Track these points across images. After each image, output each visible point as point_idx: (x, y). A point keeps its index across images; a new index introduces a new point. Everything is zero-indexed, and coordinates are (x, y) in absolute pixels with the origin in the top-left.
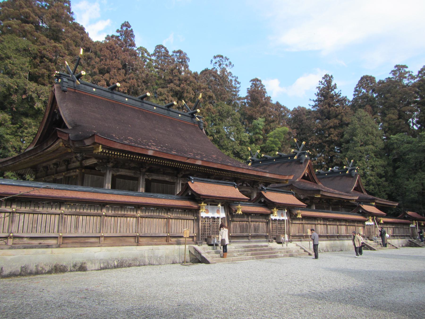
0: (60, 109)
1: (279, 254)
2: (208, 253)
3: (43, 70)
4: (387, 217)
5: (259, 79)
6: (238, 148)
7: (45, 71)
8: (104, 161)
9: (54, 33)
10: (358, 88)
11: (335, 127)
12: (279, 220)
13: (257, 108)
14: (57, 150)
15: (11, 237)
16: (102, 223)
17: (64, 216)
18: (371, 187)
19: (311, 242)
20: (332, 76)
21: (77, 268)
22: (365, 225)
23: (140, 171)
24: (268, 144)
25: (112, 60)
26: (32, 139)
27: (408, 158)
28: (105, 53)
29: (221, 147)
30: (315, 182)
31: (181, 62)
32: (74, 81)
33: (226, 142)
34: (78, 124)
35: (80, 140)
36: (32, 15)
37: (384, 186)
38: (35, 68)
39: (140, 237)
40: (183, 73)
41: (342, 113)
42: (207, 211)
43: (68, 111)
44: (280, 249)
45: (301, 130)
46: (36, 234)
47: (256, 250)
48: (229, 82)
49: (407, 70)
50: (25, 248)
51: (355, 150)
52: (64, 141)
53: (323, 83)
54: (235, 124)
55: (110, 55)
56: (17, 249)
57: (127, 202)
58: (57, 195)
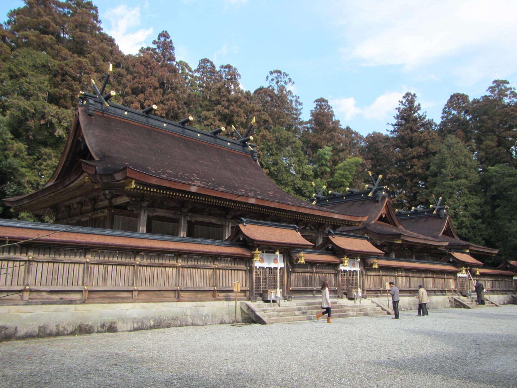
0: (85, 137)
1: (351, 313)
2: (264, 311)
3: (65, 90)
4: (484, 267)
5: (326, 99)
6: (300, 183)
7: (68, 91)
8: (138, 199)
9: (78, 45)
10: (447, 109)
11: (419, 157)
12: (350, 271)
13: (323, 135)
14: (82, 186)
15: (27, 291)
16: (135, 275)
17: (90, 265)
18: (465, 230)
19: (391, 299)
20: (414, 95)
21: (106, 328)
22: (457, 277)
23: (181, 212)
24: (336, 178)
25: (147, 78)
26: (52, 173)
27: (510, 195)
28: (139, 69)
29: (279, 182)
30: (395, 225)
31: (231, 79)
32: (102, 103)
33: (285, 176)
34: (106, 154)
35: (110, 174)
36: (52, 24)
37: (480, 230)
38: (55, 88)
39: (182, 291)
40: (233, 93)
41: (427, 139)
42: (262, 260)
43: (94, 139)
44: (352, 307)
45: (377, 162)
46: (57, 287)
48: (288, 103)
49: (508, 86)
50: (43, 304)
51: (444, 186)
52: (90, 175)
53: (404, 103)
54: (296, 154)
55: (145, 72)
56: (34, 305)
57: (166, 249)
58: (82, 241)
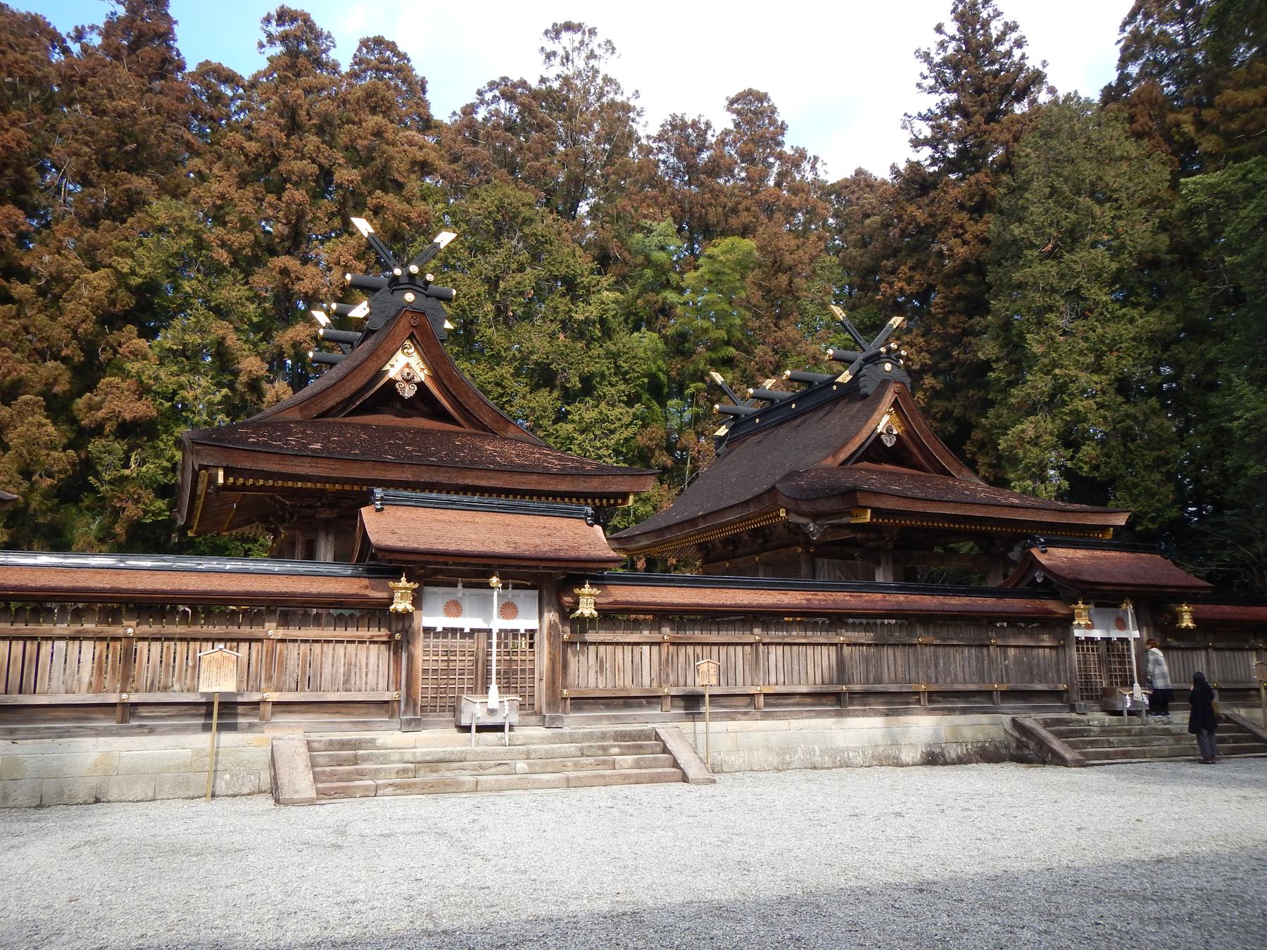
5: (762, 90)
30: (484, 428)
51: (1021, 286)
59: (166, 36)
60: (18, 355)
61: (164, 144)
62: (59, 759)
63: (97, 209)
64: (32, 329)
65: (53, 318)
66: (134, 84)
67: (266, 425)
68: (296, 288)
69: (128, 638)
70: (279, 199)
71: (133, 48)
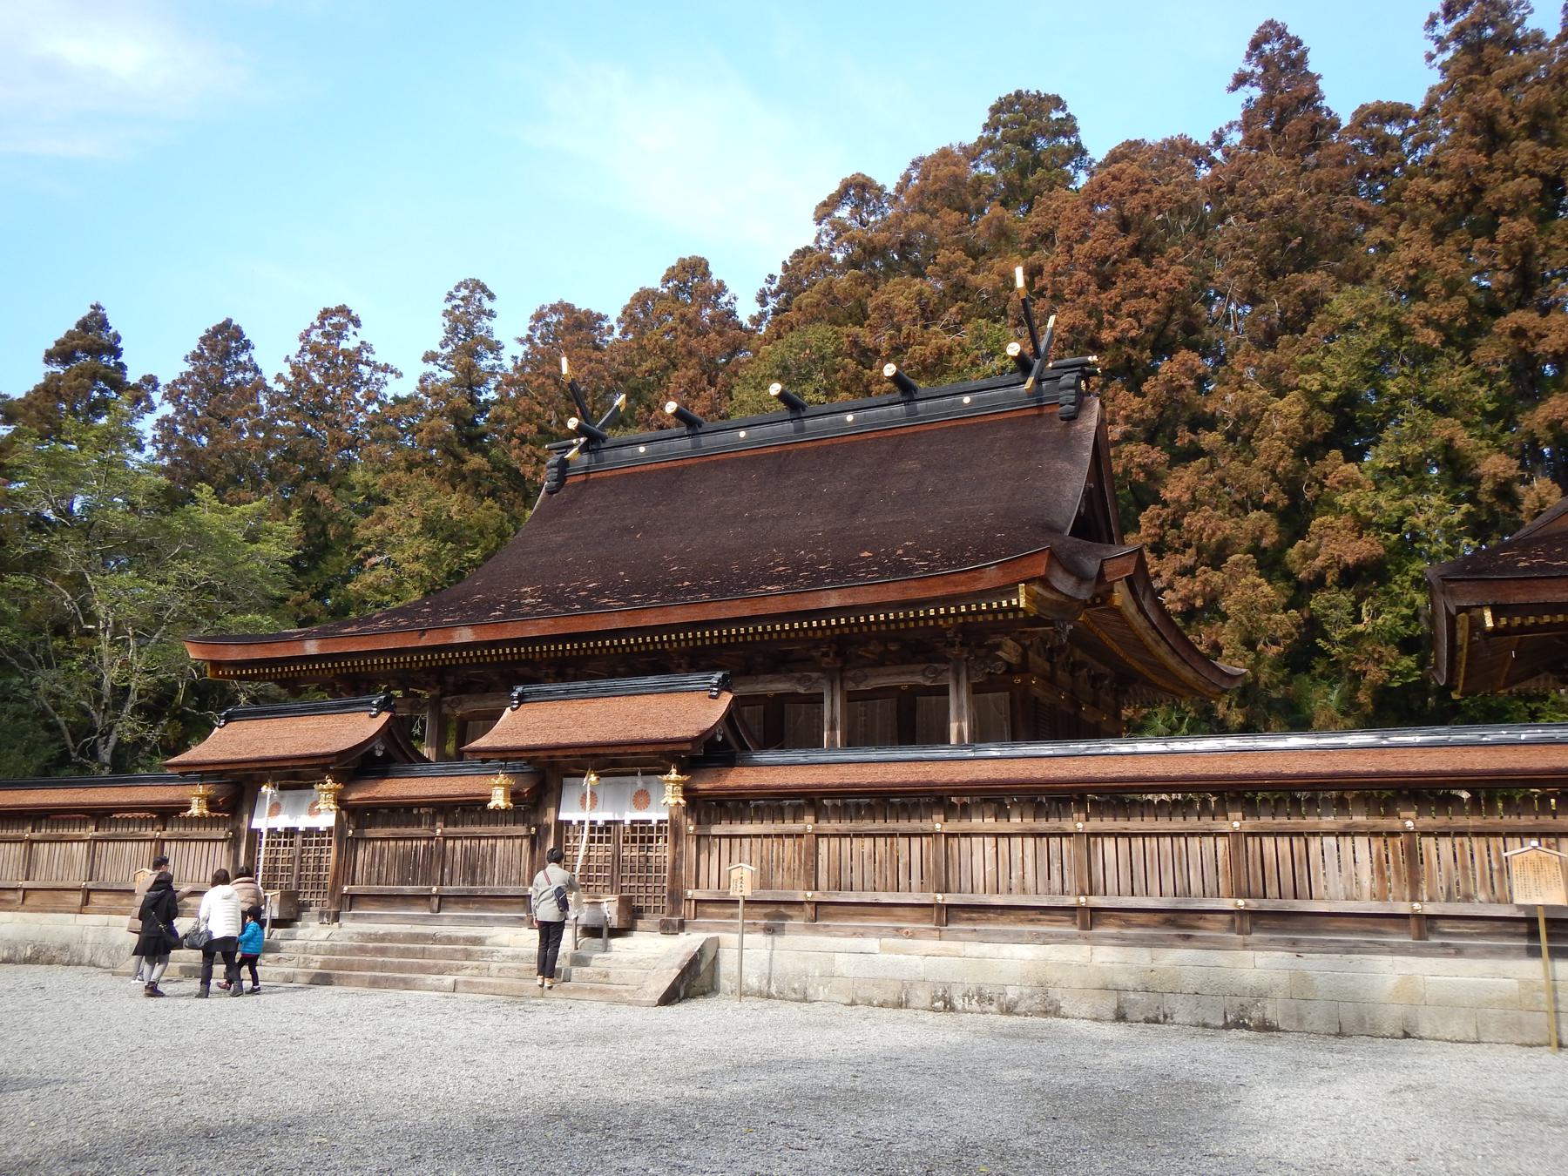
42: (276, 808)
47: (382, 952)
59: (1310, 98)
60: (1219, 513)
61: (1334, 225)
62: (1352, 979)
63: (1271, 326)
64: (1228, 481)
65: (1247, 463)
66: (1286, 168)
67: (1537, 541)
68: (1539, 349)
69: (1408, 832)
70: (1493, 240)
71: (1277, 129)
